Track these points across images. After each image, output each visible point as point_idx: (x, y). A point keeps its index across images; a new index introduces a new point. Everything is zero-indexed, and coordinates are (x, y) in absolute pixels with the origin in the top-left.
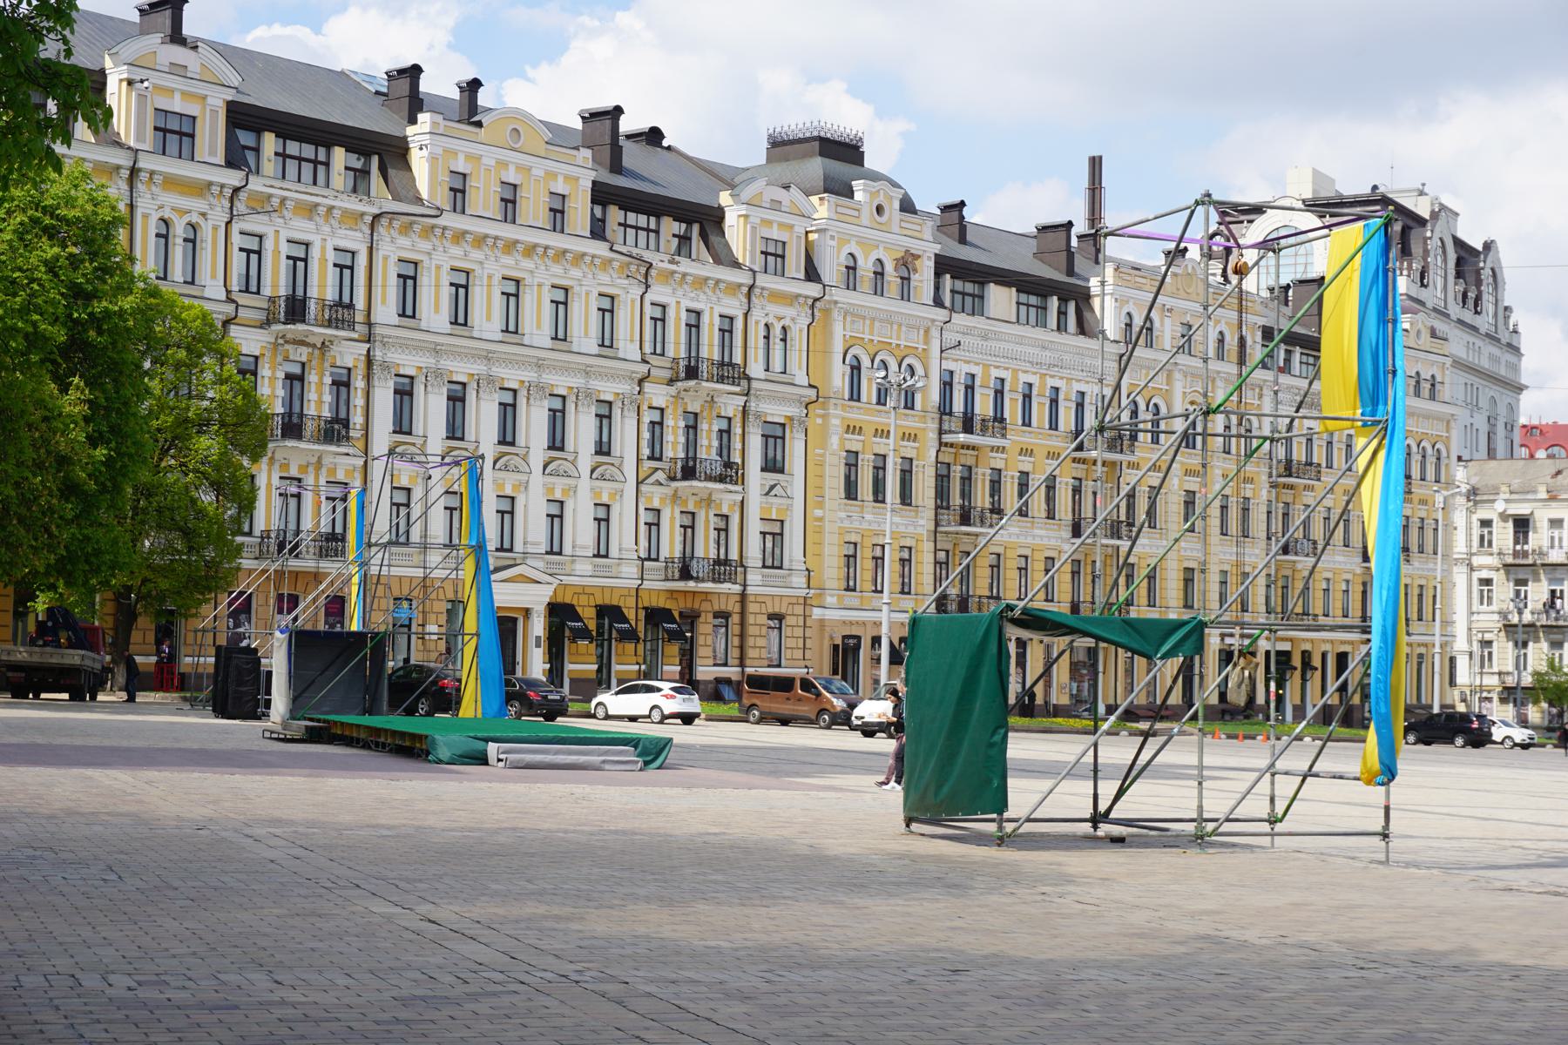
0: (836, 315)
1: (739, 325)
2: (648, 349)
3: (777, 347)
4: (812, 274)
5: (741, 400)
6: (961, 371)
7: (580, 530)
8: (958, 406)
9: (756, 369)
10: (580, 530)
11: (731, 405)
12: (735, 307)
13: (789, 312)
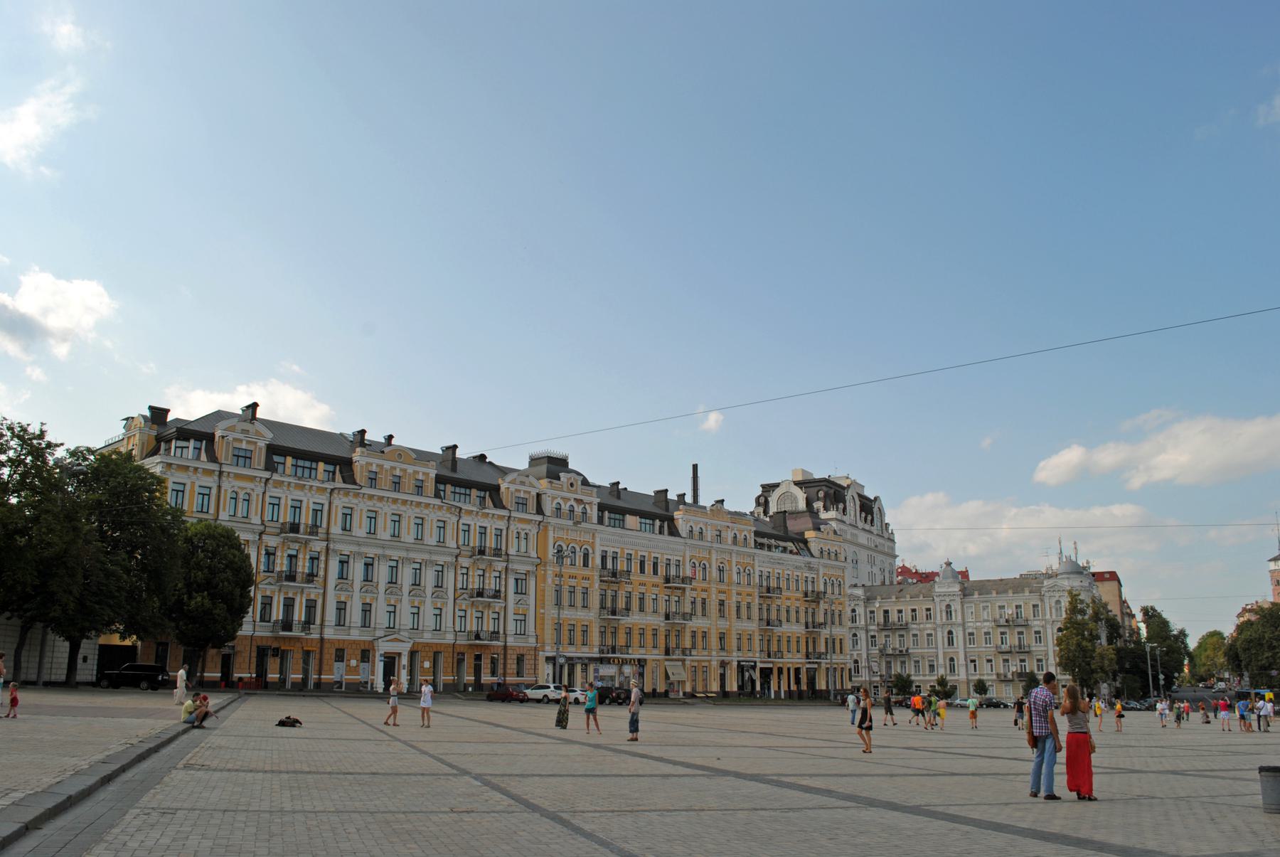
0: (550, 528)
1: (504, 533)
2: (461, 543)
3: (523, 543)
4: (540, 511)
5: (505, 564)
6: (610, 550)
7: (428, 620)
8: (609, 565)
9: (512, 551)
10: (428, 620)
11: (500, 566)
12: (502, 525)
13: (527, 527)
